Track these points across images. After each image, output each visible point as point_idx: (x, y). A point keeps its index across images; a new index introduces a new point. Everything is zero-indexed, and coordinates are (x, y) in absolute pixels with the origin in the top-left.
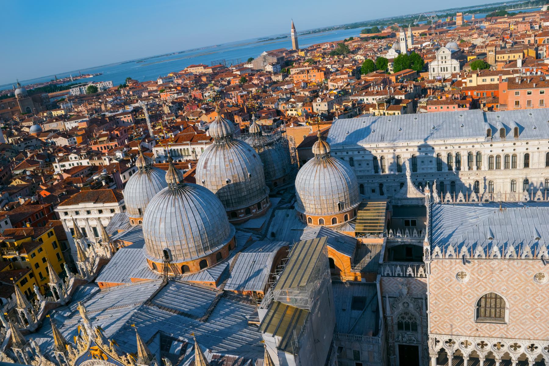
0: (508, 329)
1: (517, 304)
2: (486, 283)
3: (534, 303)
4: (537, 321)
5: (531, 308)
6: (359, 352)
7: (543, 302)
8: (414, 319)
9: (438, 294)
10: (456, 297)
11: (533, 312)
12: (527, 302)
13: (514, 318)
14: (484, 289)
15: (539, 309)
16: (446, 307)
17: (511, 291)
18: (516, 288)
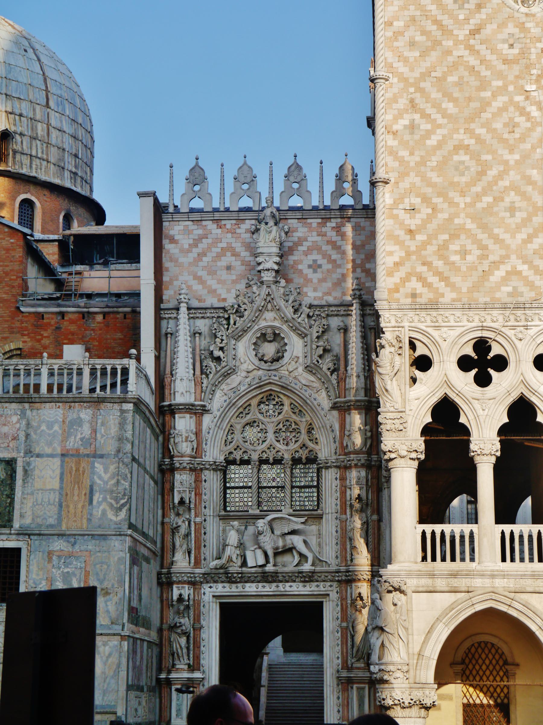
6: (10, 464)
8: (304, 437)
9: (424, 76)
10: (503, 90)
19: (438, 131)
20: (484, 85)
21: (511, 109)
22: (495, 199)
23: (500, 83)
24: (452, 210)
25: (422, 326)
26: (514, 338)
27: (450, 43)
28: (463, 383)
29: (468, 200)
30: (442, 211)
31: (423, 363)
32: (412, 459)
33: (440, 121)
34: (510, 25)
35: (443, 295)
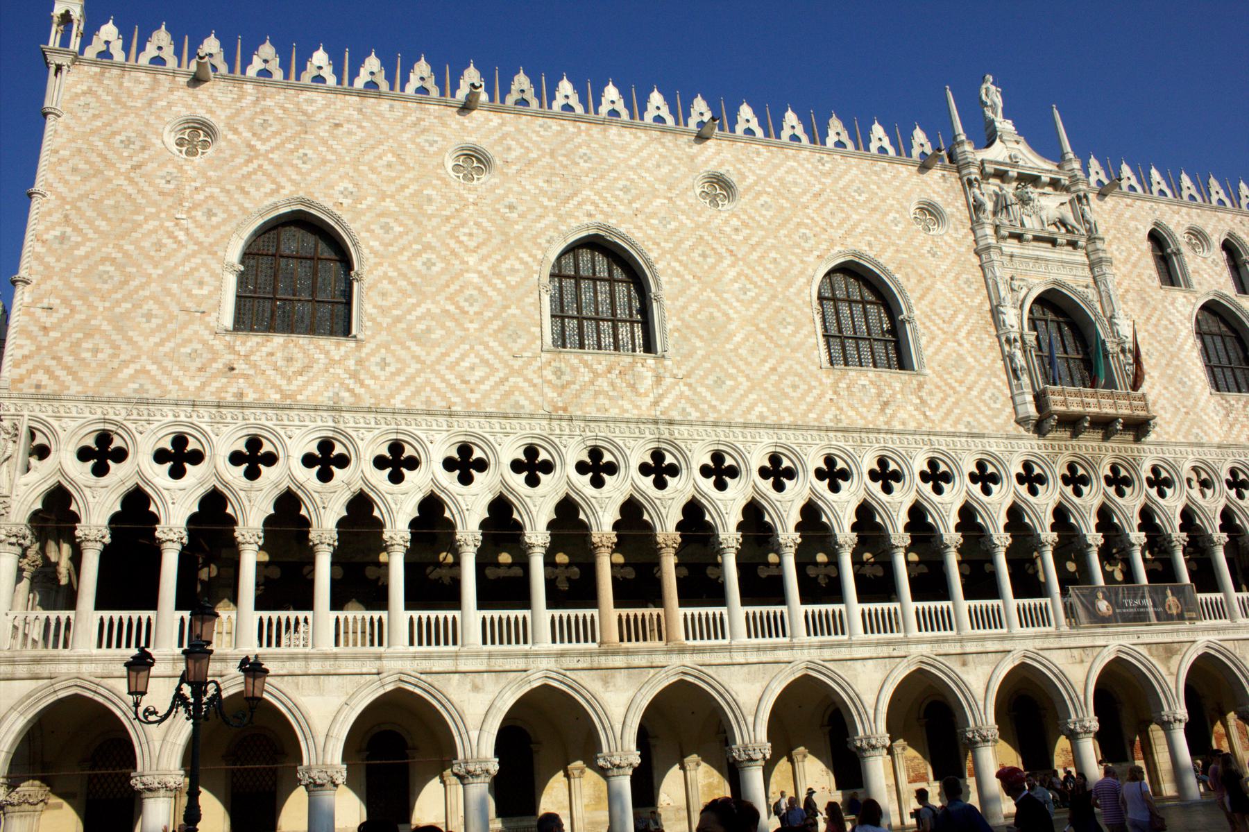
0: (360, 362)
1: (395, 254)
2: (278, 166)
3: (453, 252)
4: (473, 327)
5: (443, 271)
7: (484, 251)
9: (81, 197)
10: (156, 216)
11: (453, 288)
12: (428, 247)
13: (383, 311)
14: (269, 187)
15: (474, 277)
16: (103, 260)
17: (370, 200)
18: (389, 189)
19: (88, 244)
20: (138, 210)
21: (161, 232)
22: (133, 306)
23: (153, 210)
24: (91, 312)
25: (42, 416)
26: (134, 431)
27: (112, 173)
28: (80, 472)
29: (107, 304)
30: (80, 312)
31: (42, 452)
32: (12, 544)
33: (91, 235)
34: (170, 166)
35: (68, 388)
